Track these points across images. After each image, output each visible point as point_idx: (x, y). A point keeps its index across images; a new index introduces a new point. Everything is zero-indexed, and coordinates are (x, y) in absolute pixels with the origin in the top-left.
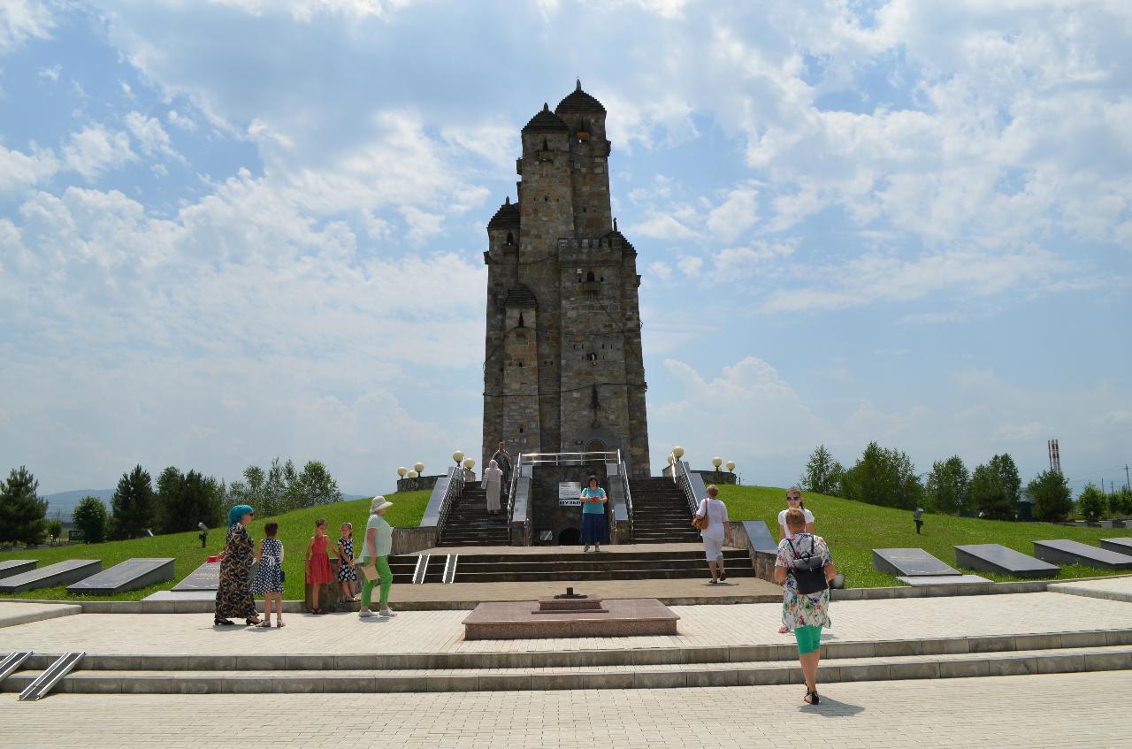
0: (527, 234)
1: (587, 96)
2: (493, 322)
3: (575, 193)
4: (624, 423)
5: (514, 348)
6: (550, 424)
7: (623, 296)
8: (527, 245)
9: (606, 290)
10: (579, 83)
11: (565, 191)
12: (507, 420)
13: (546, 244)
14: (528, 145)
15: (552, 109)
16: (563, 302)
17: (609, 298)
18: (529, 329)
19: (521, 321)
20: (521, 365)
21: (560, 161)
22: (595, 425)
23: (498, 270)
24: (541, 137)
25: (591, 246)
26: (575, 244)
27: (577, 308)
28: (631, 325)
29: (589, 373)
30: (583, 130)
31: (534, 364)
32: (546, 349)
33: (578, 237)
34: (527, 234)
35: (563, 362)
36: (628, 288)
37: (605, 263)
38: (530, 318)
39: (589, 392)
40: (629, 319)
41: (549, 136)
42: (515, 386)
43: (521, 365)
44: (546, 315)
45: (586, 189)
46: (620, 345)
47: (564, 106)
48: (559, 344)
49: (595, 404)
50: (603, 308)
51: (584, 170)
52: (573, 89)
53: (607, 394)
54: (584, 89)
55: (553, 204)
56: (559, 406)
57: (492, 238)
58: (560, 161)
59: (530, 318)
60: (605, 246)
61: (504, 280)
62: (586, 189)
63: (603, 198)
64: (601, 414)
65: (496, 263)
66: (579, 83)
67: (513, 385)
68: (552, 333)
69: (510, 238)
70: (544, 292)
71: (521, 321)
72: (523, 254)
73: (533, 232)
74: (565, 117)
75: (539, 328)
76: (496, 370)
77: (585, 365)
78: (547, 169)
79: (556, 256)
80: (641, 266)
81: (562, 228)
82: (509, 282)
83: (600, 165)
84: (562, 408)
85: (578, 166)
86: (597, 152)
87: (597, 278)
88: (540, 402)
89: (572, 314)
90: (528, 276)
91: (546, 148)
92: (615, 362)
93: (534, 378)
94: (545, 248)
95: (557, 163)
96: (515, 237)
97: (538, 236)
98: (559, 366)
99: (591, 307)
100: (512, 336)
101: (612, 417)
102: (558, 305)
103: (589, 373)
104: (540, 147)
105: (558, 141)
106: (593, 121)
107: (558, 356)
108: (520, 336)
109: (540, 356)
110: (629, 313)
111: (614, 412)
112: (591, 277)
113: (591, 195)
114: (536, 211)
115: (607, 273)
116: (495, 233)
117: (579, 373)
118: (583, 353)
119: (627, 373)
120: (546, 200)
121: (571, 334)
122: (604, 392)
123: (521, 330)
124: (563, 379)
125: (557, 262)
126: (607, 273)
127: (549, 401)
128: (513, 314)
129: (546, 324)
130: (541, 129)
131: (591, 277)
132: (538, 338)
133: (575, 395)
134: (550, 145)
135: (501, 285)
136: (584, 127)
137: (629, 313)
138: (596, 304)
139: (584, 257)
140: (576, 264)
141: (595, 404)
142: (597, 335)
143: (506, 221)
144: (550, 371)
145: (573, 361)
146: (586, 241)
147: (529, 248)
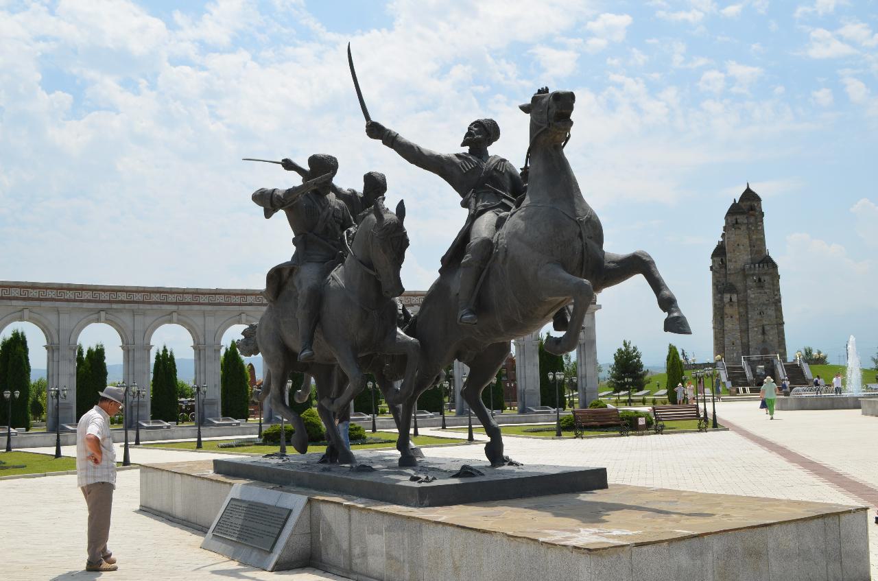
0: (730, 261)
1: (752, 192)
2: (717, 297)
3: (750, 239)
4: (776, 340)
5: (728, 310)
6: (745, 341)
7: (773, 285)
8: (730, 266)
9: (767, 285)
10: (748, 184)
11: (746, 241)
12: (726, 340)
13: (739, 265)
14: (729, 221)
15: (737, 202)
16: (749, 291)
17: (768, 288)
18: (734, 302)
19: (731, 299)
20: (732, 317)
21: (744, 228)
22: (764, 341)
23: (718, 275)
24: (735, 217)
25: (759, 266)
26: (753, 266)
27: (754, 294)
28: (777, 298)
29: (761, 320)
30: (752, 210)
31: (737, 316)
32: (742, 310)
33: (753, 263)
34: (730, 261)
35: (750, 316)
36: (775, 282)
37: (765, 274)
38: (735, 298)
39: (761, 328)
40: (776, 295)
41: (738, 217)
42: (730, 326)
43: (732, 317)
44: (741, 295)
45: (754, 237)
46: (773, 308)
47: (742, 199)
48: (747, 308)
49: (764, 333)
50: (766, 293)
51: (753, 228)
52: (745, 188)
53: (768, 328)
54: (752, 188)
55: (741, 247)
56: (748, 333)
57: (714, 262)
58: (744, 228)
59: (735, 298)
60: (766, 267)
61: (720, 279)
62: (754, 237)
63: (762, 240)
64: (766, 337)
65: (716, 272)
66: (748, 184)
67: (729, 325)
68: (744, 303)
69: (722, 260)
70: (739, 286)
71: (731, 299)
72: (729, 269)
73: (733, 260)
74: (743, 205)
75: (738, 300)
76: (719, 318)
77: (759, 317)
78: (738, 232)
79: (744, 269)
80: (780, 271)
81: (746, 258)
82: (722, 280)
83: (761, 225)
84: (750, 335)
85: (750, 226)
86: (759, 220)
87: (762, 280)
88: (741, 332)
89: (753, 296)
90: (732, 279)
91: (737, 223)
92: (771, 316)
93: (738, 322)
94: (738, 267)
95: (742, 229)
96: (724, 260)
97: (736, 262)
98: (748, 317)
99: (760, 293)
100: (727, 306)
101: (771, 338)
102: (746, 291)
103: (761, 320)
104: (734, 222)
105: (742, 219)
106: (756, 205)
107: (747, 312)
108: (731, 305)
109: (739, 313)
110: (776, 293)
111: (772, 336)
112: (760, 280)
113: (757, 239)
114: (734, 250)
115: (767, 278)
116: (715, 259)
117: (756, 320)
118: (758, 312)
119: (776, 318)
120: (738, 245)
121: (752, 304)
122: (767, 328)
123: (731, 303)
124: (750, 323)
125: (744, 273)
126: (767, 278)
127: (745, 331)
128: (727, 297)
129: (741, 299)
130: (734, 211)
131: (760, 280)
132: (738, 306)
133: (756, 329)
134: (738, 220)
135: (719, 282)
136: (752, 208)
137: (776, 293)
138: (762, 291)
139: (757, 272)
140: (753, 275)
141: (764, 333)
142: (764, 304)
143: (719, 252)
144: (744, 319)
145: (753, 315)
146: (757, 265)
147: (732, 267)
